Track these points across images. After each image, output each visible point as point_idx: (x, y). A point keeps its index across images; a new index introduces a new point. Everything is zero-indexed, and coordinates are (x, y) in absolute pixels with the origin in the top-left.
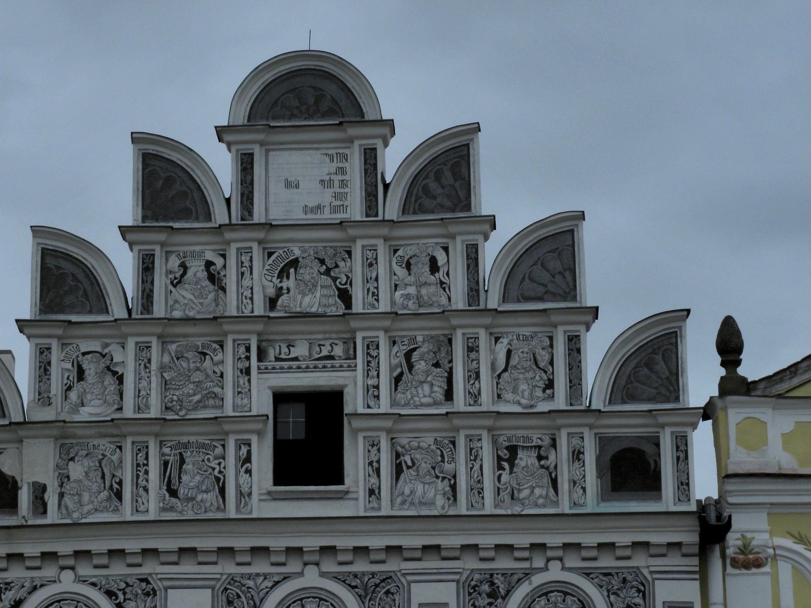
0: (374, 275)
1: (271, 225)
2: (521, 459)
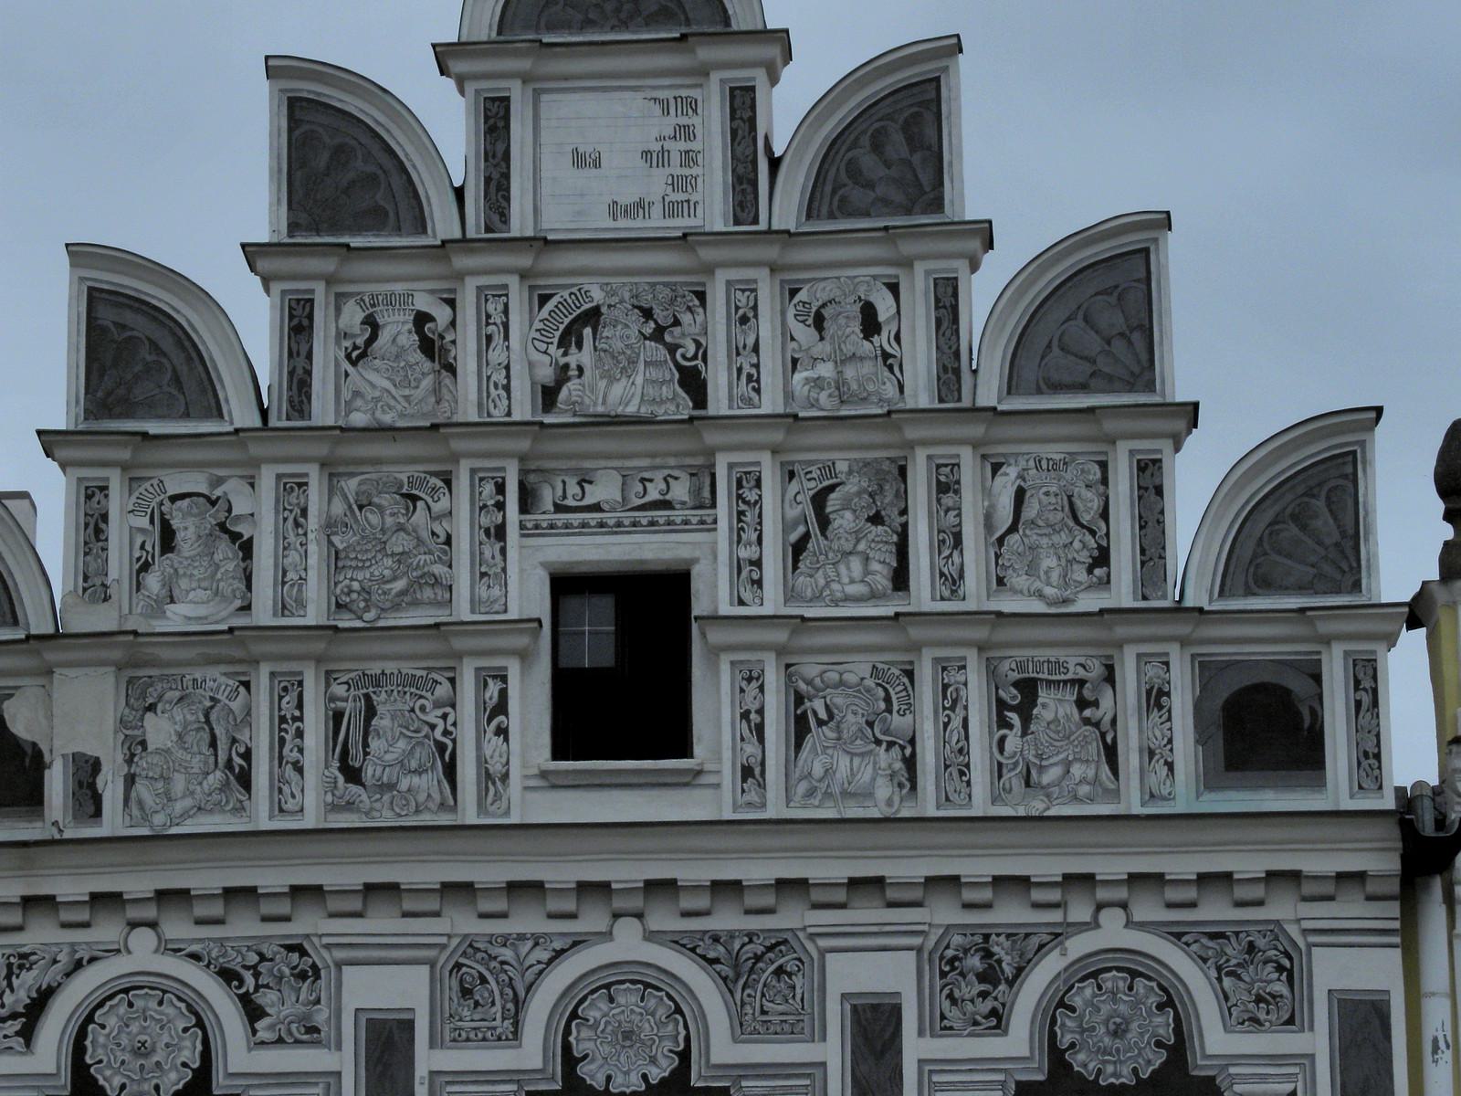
0: (751, 341)
1: (545, 239)
2: (1044, 706)
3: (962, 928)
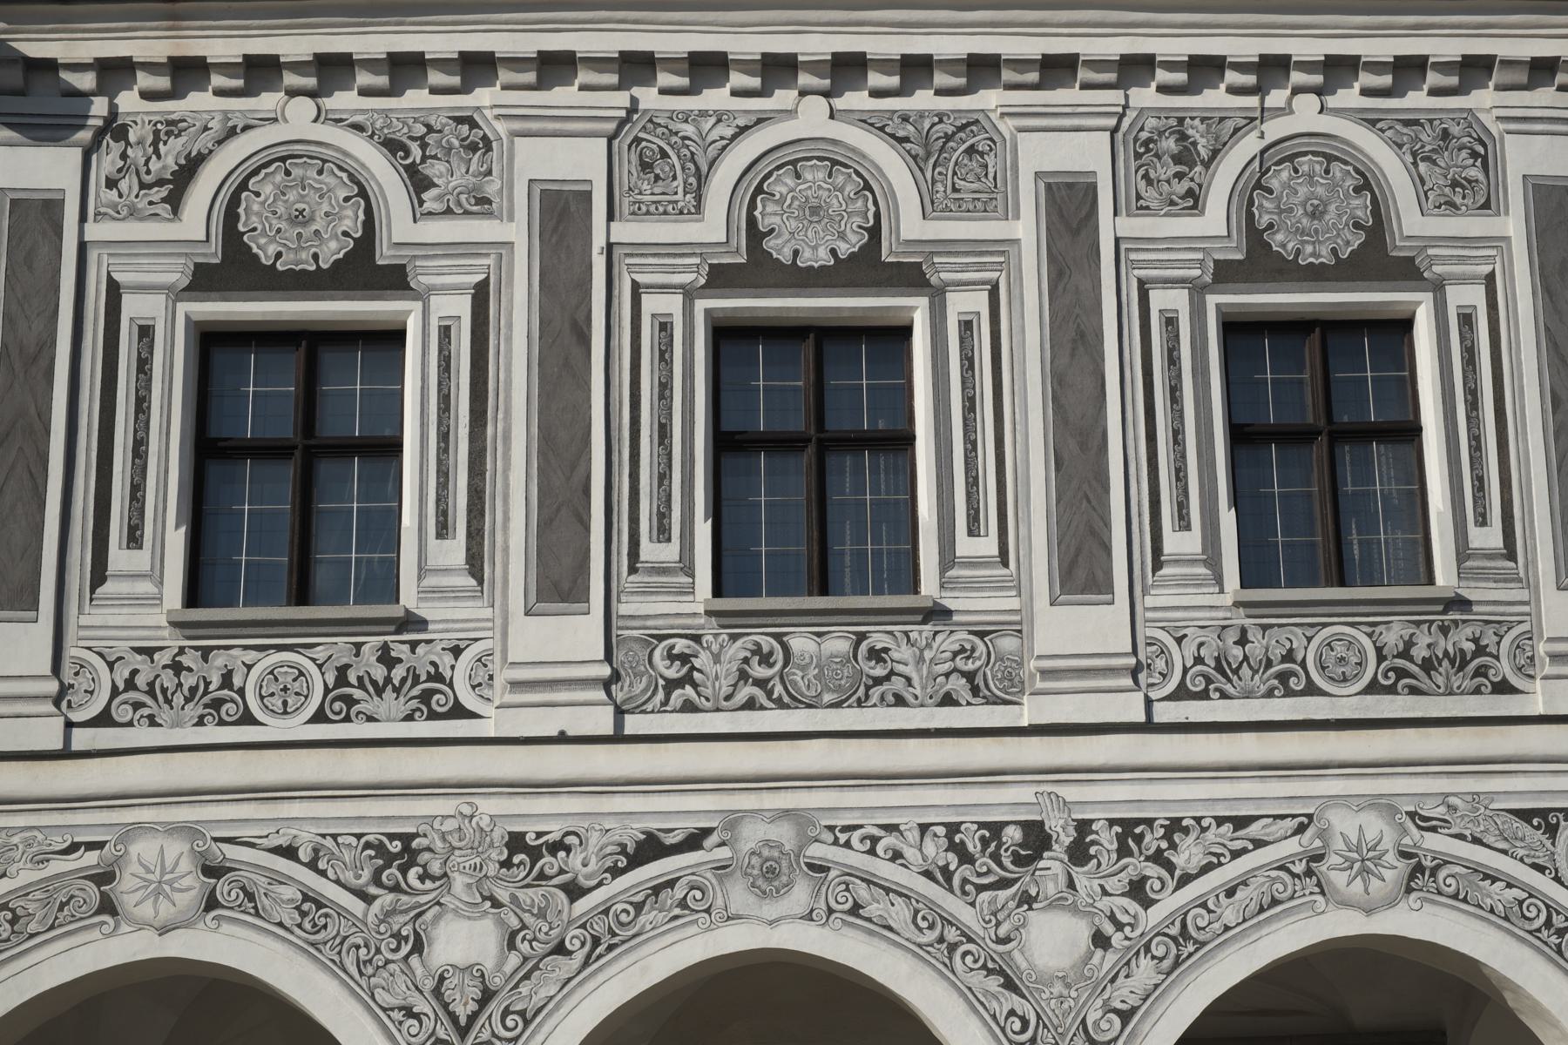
3: (1158, 112)
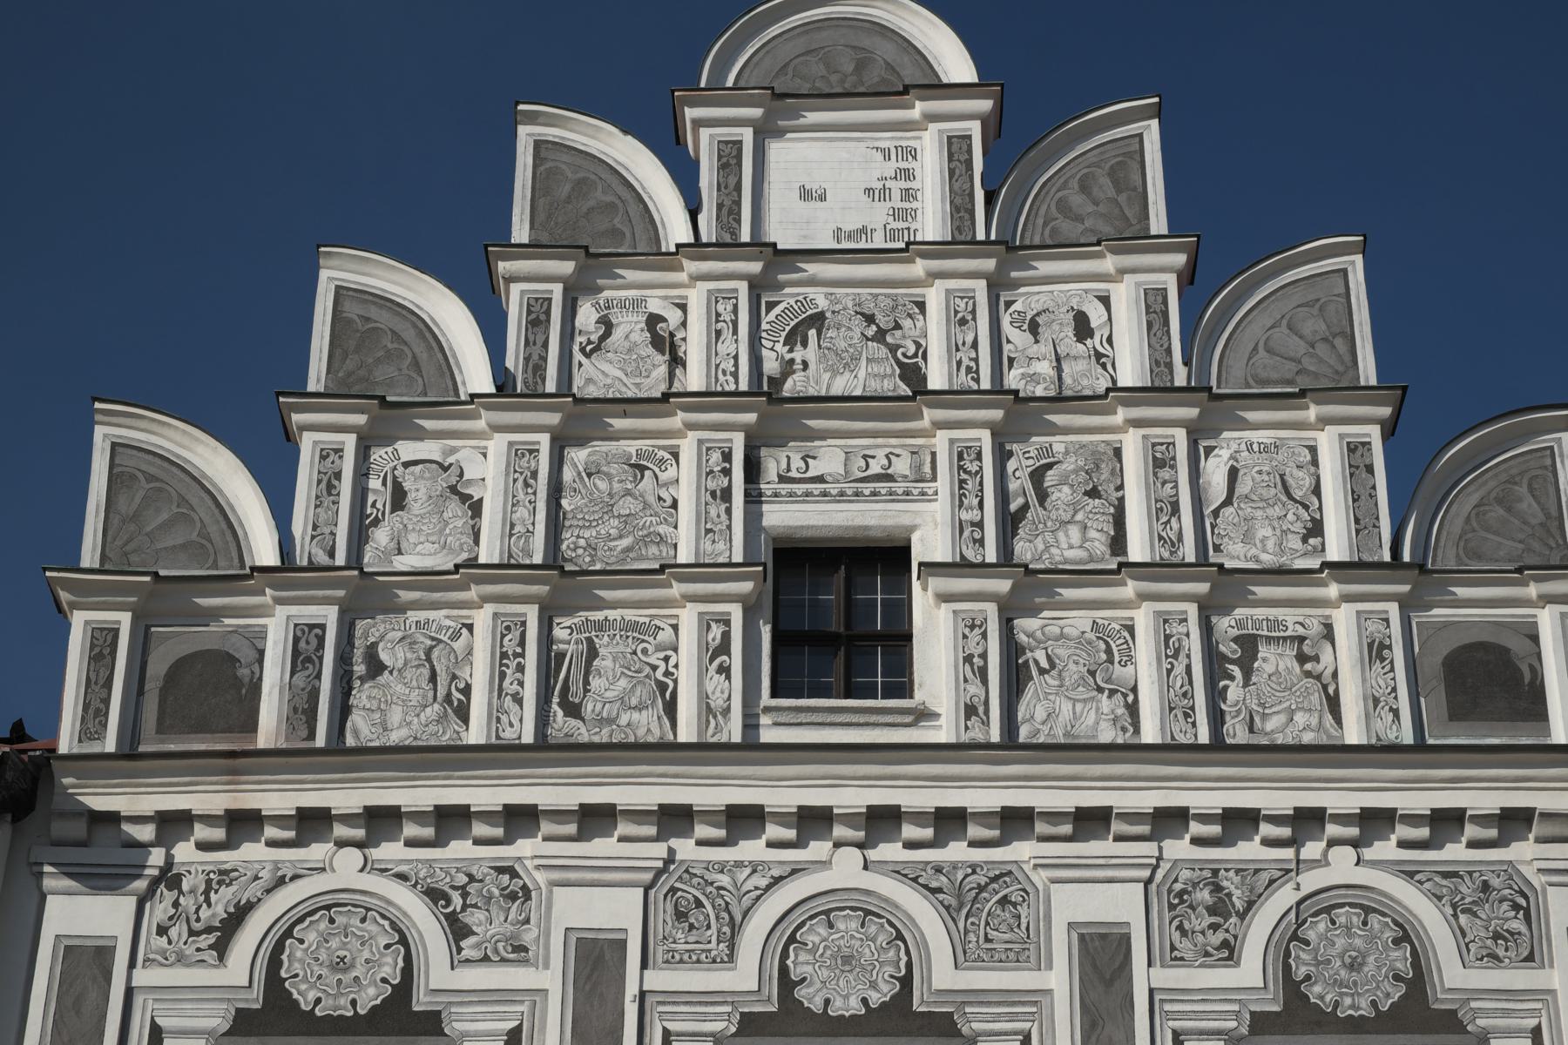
0: (970, 339)
3: (1192, 864)
